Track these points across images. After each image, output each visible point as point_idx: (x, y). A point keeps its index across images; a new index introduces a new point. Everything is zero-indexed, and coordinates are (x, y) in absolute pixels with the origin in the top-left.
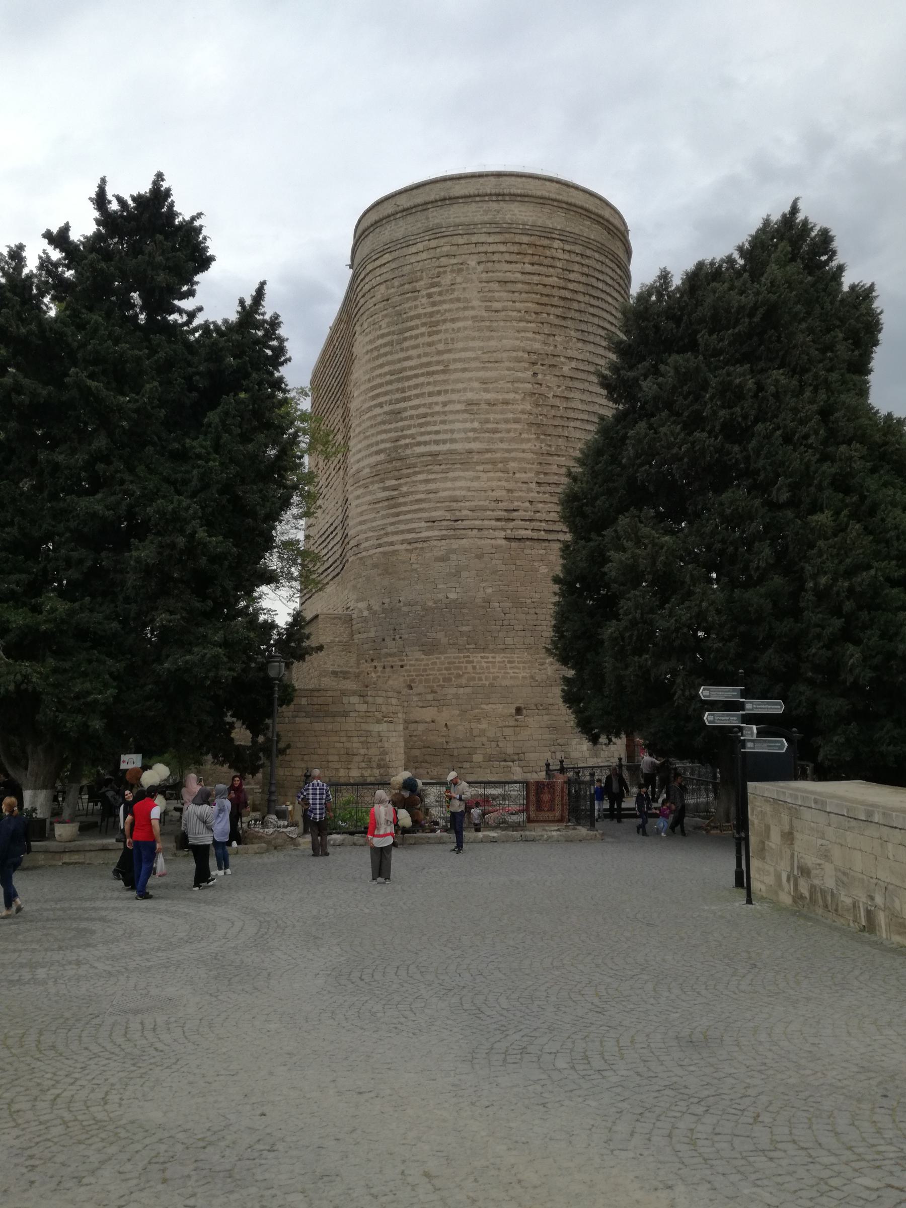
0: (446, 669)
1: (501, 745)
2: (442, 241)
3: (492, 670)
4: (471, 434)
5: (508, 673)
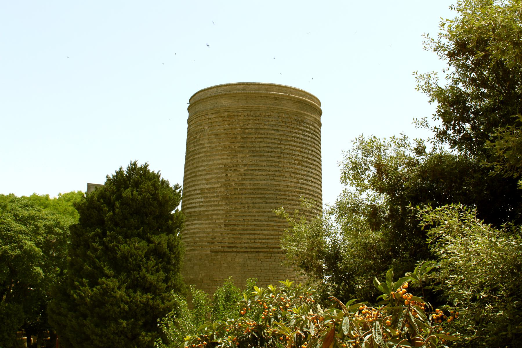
2: (199, 118)
4: (201, 204)
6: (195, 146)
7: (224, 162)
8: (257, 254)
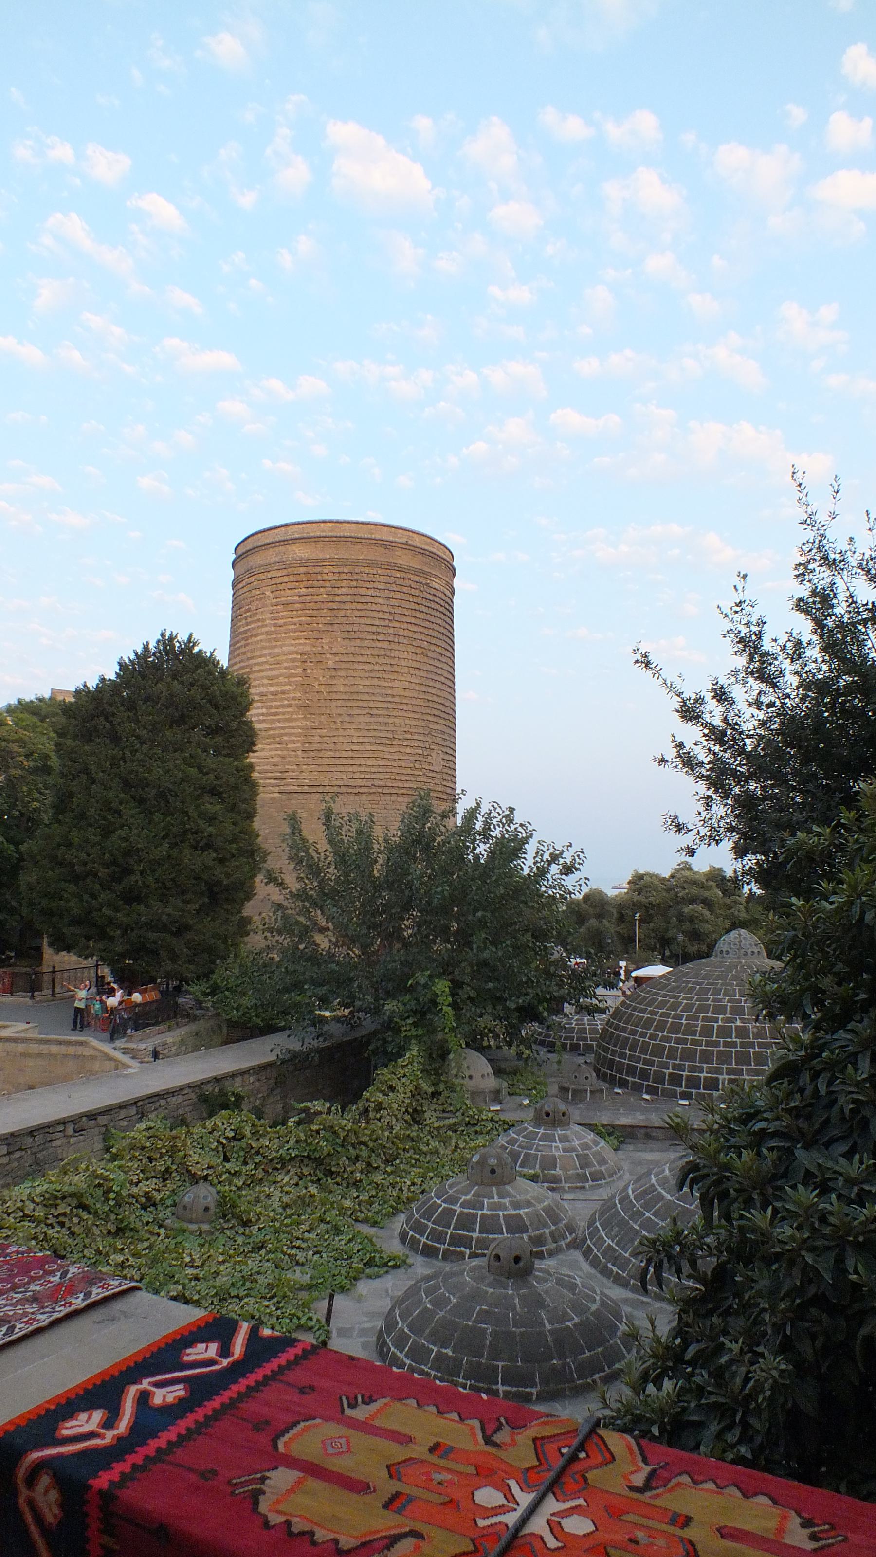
4: (261, 718)
6: (247, 624)
7: (301, 649)
8: (357, 798)
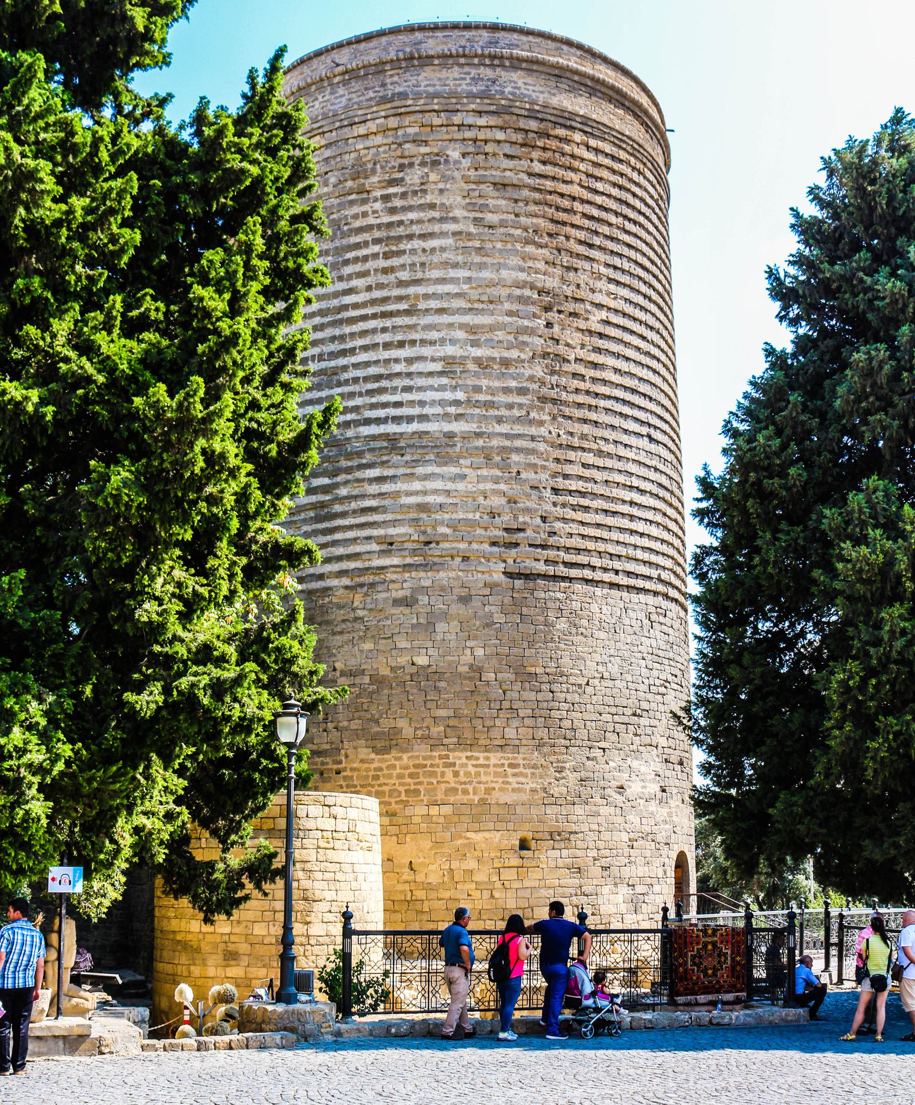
0: (411, 775)
1: (497, 894)
3: (483, 778)
4: (452, 410)
5: (508, 783)
